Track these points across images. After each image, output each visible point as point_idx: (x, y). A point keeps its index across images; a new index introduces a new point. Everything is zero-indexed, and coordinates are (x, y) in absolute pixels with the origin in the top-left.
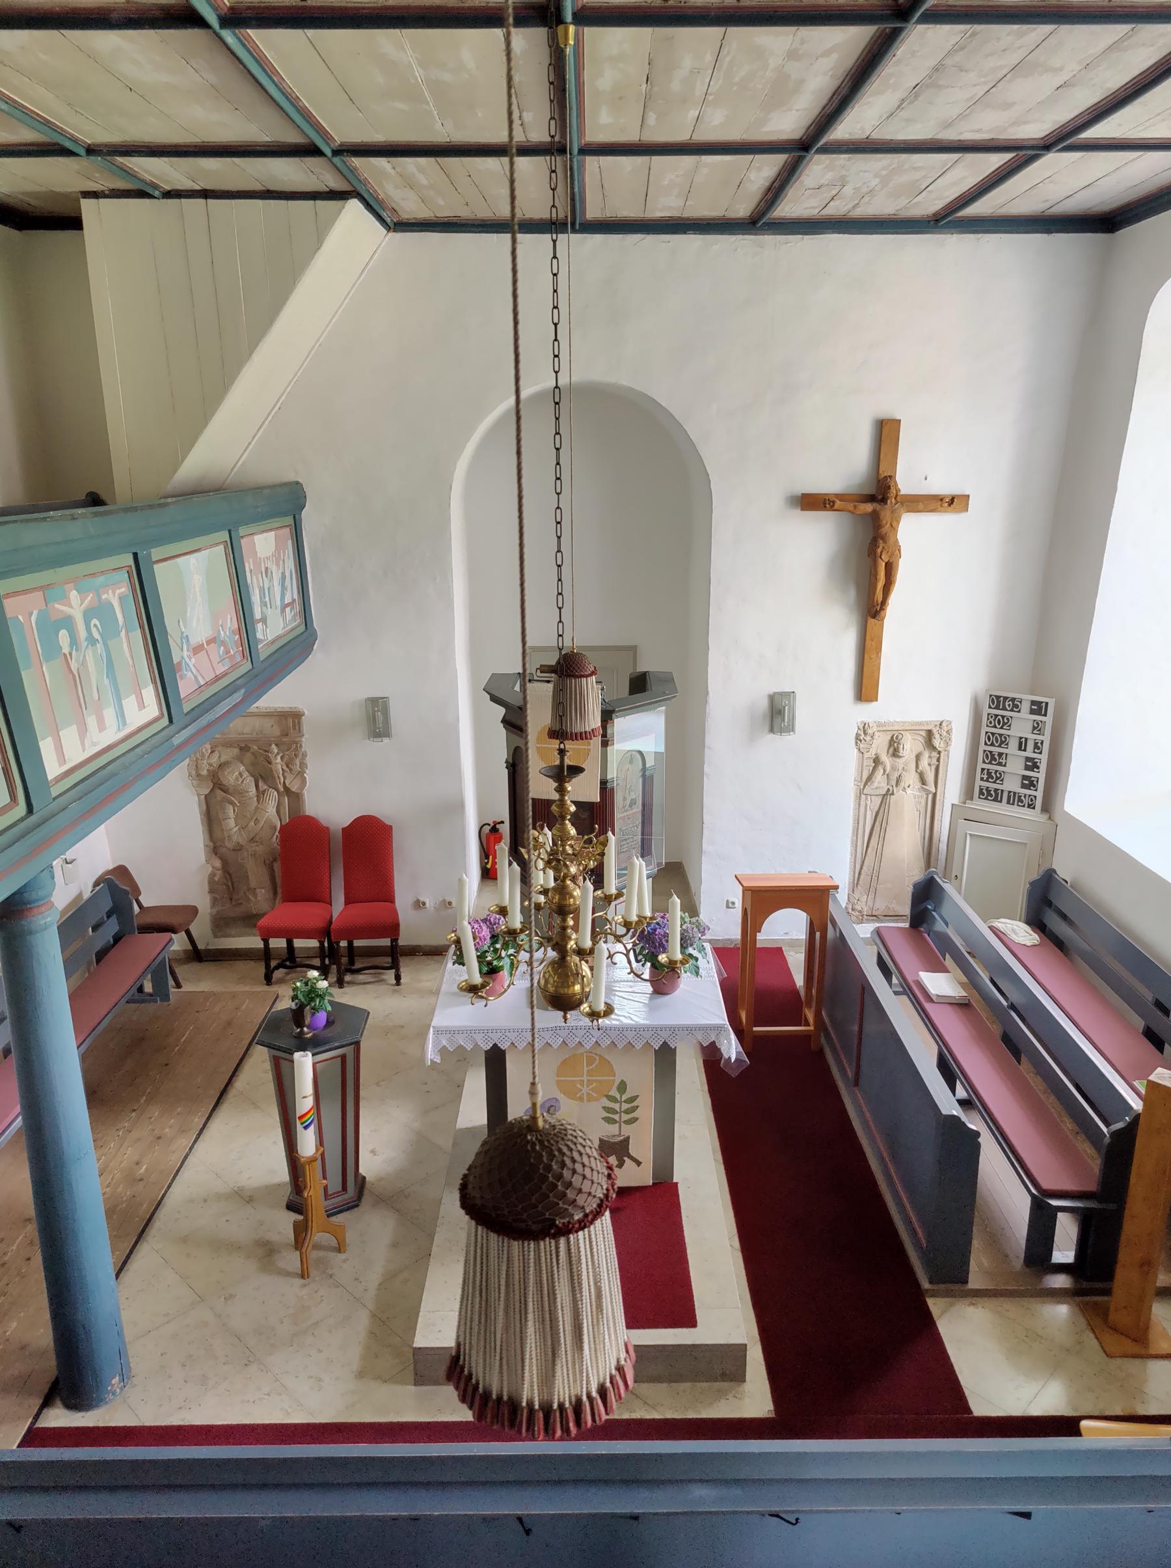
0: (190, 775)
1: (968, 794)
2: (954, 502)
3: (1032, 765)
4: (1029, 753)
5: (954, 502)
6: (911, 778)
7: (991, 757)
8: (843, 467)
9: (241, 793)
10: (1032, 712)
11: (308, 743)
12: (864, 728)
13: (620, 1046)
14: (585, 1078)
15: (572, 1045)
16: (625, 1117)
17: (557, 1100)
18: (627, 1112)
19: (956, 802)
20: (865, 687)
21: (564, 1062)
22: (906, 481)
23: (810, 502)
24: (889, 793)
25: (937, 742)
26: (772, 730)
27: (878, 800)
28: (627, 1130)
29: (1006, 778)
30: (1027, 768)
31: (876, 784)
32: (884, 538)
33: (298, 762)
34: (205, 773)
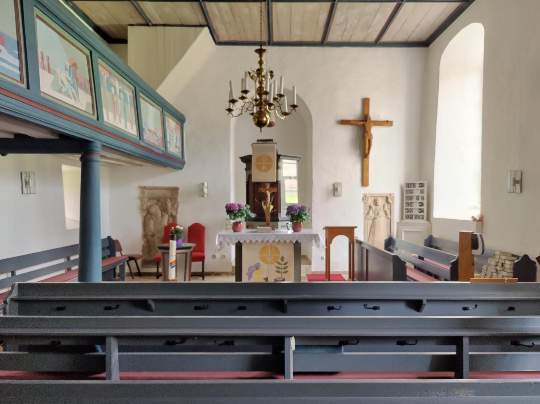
1: (402, 218)
2: (388, 123)
3: (422, 205)
4: (420, 201)
5: (388, 123)
6: (382, 213)
7: (408, 204)
8: (353, 112)
9: (156, 215)
10: (420, 187)
11: (180, 198)
12: (365, 196)
13: (282, 242)
14: (270, 255)
15: (265, 241)
16: (283, 271)
17: (259, 263)
18: (284, 268)
20: (364, 182)
21: (263, 249)
22: (374, 115)
23: (344, 122)
24: (375, 218)
25: (390, 201)
26: (334, 196)
27: (372, 221)
28: (284, 276)
29: (414, 210)
30: (420, 206)
32: (367, 132)
33: (176, 205)
34: (145, 208)
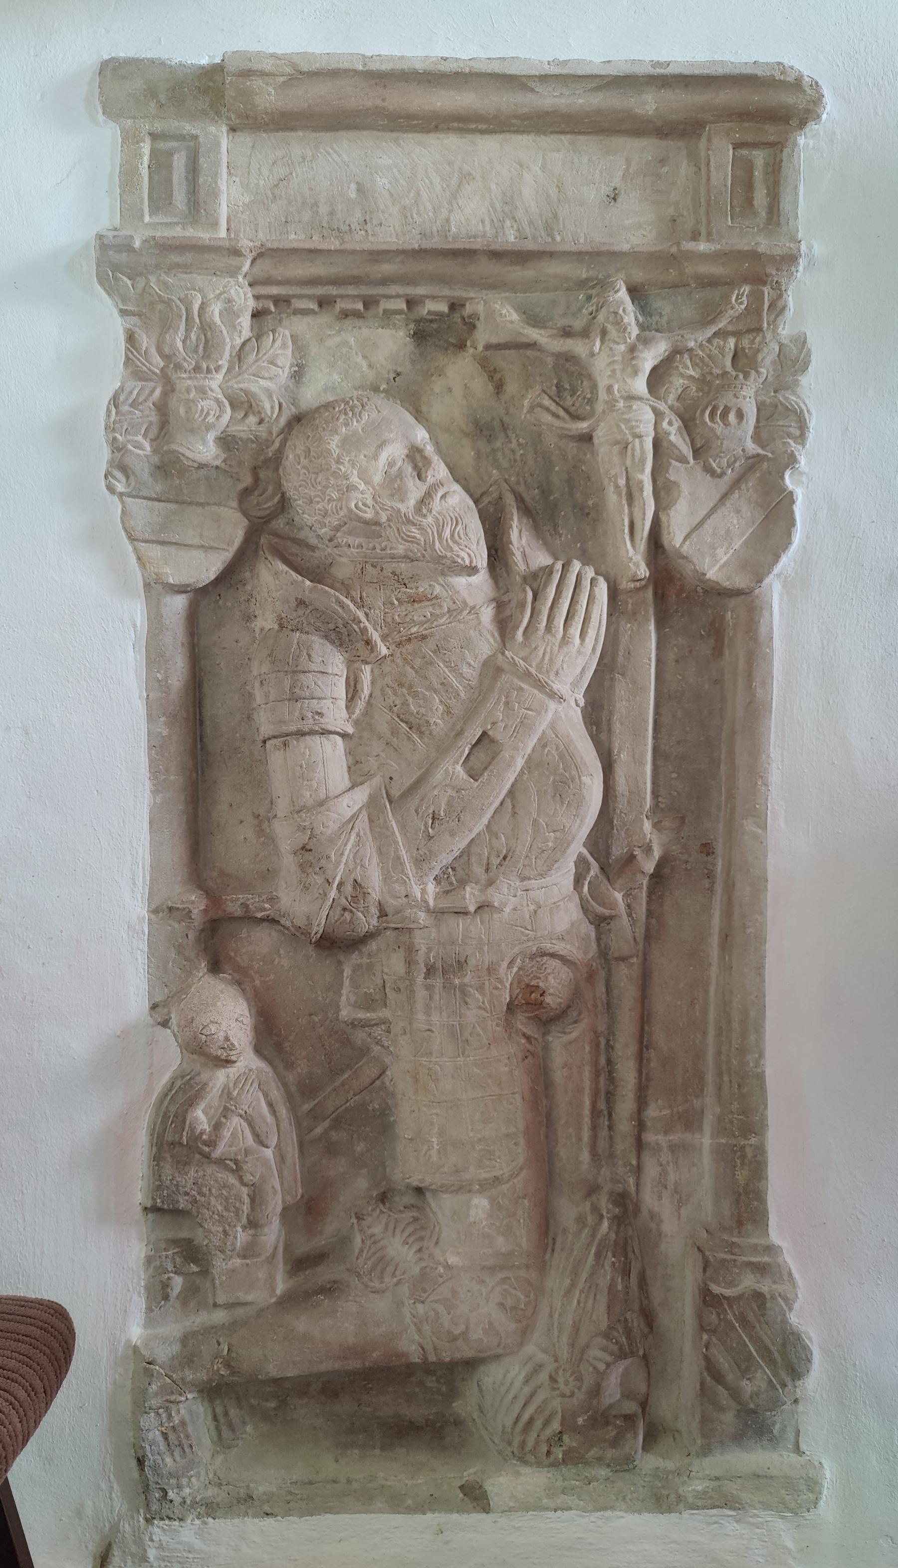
0: (121, 465)
9: (407, 572)
33: (748, 398)
34: (206, 450)
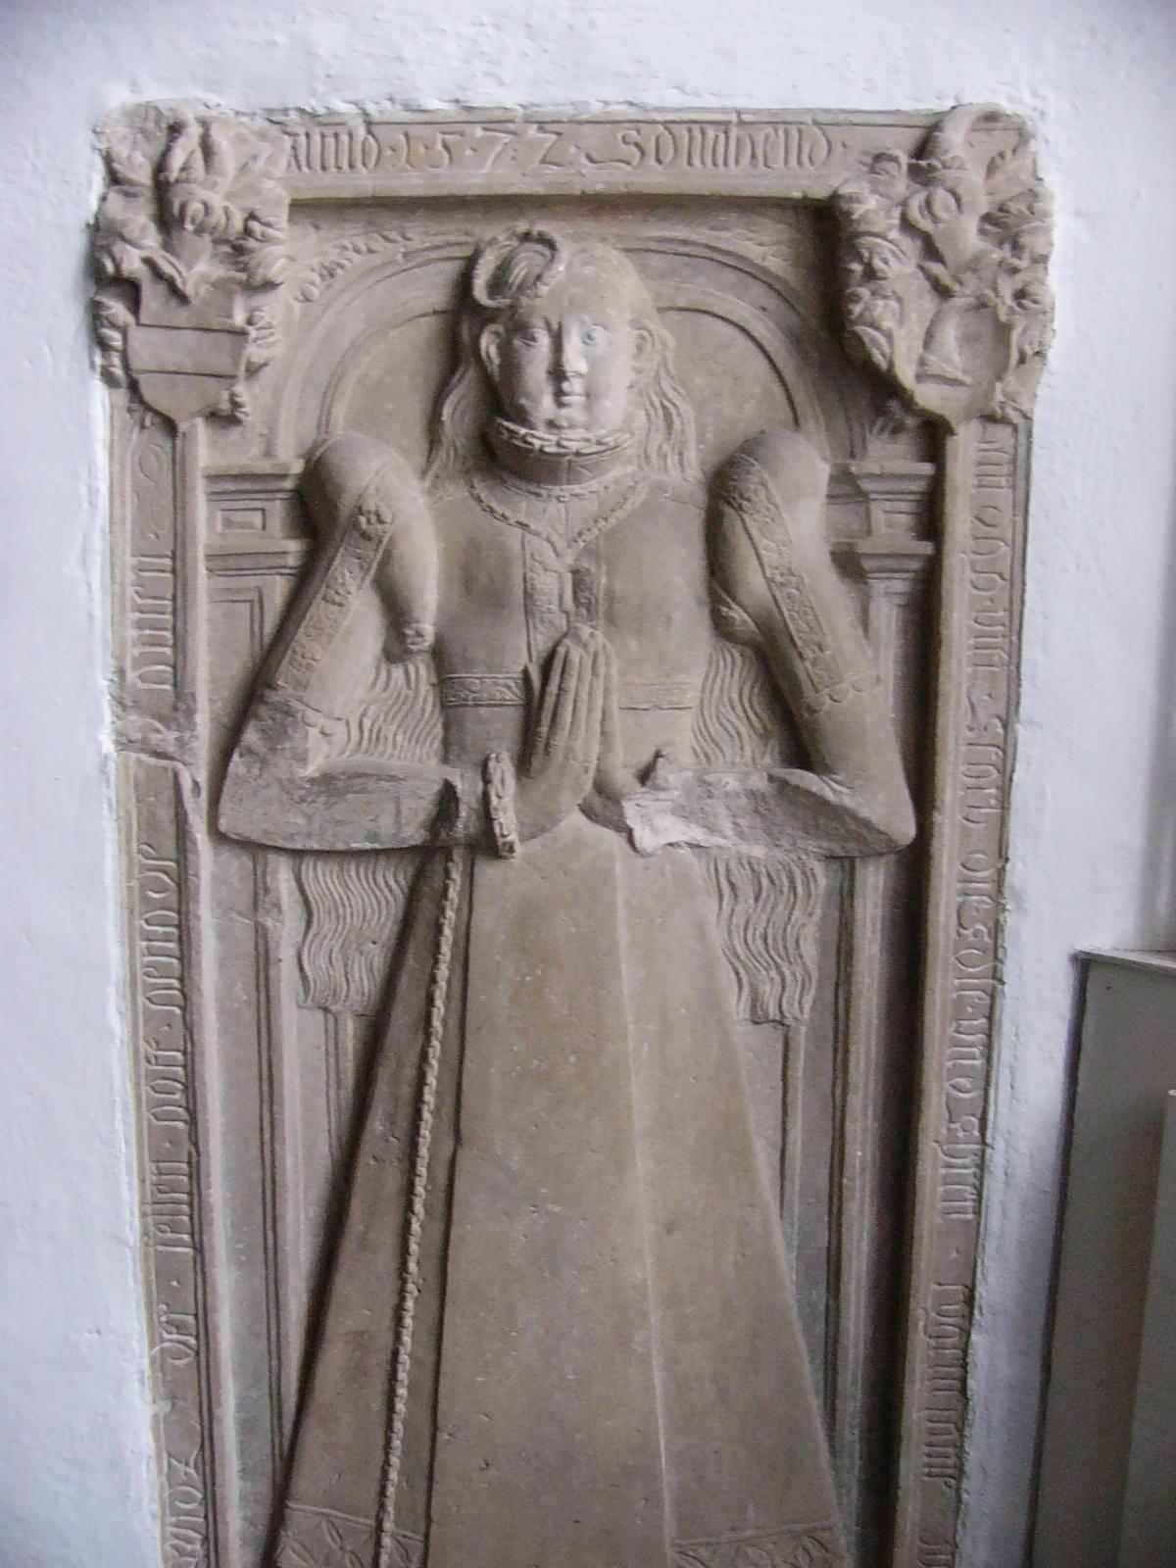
19: (1112, 932)
24: (447, 848)
25: (899, 325)
27: (371, 903)
31: (320, 751)
